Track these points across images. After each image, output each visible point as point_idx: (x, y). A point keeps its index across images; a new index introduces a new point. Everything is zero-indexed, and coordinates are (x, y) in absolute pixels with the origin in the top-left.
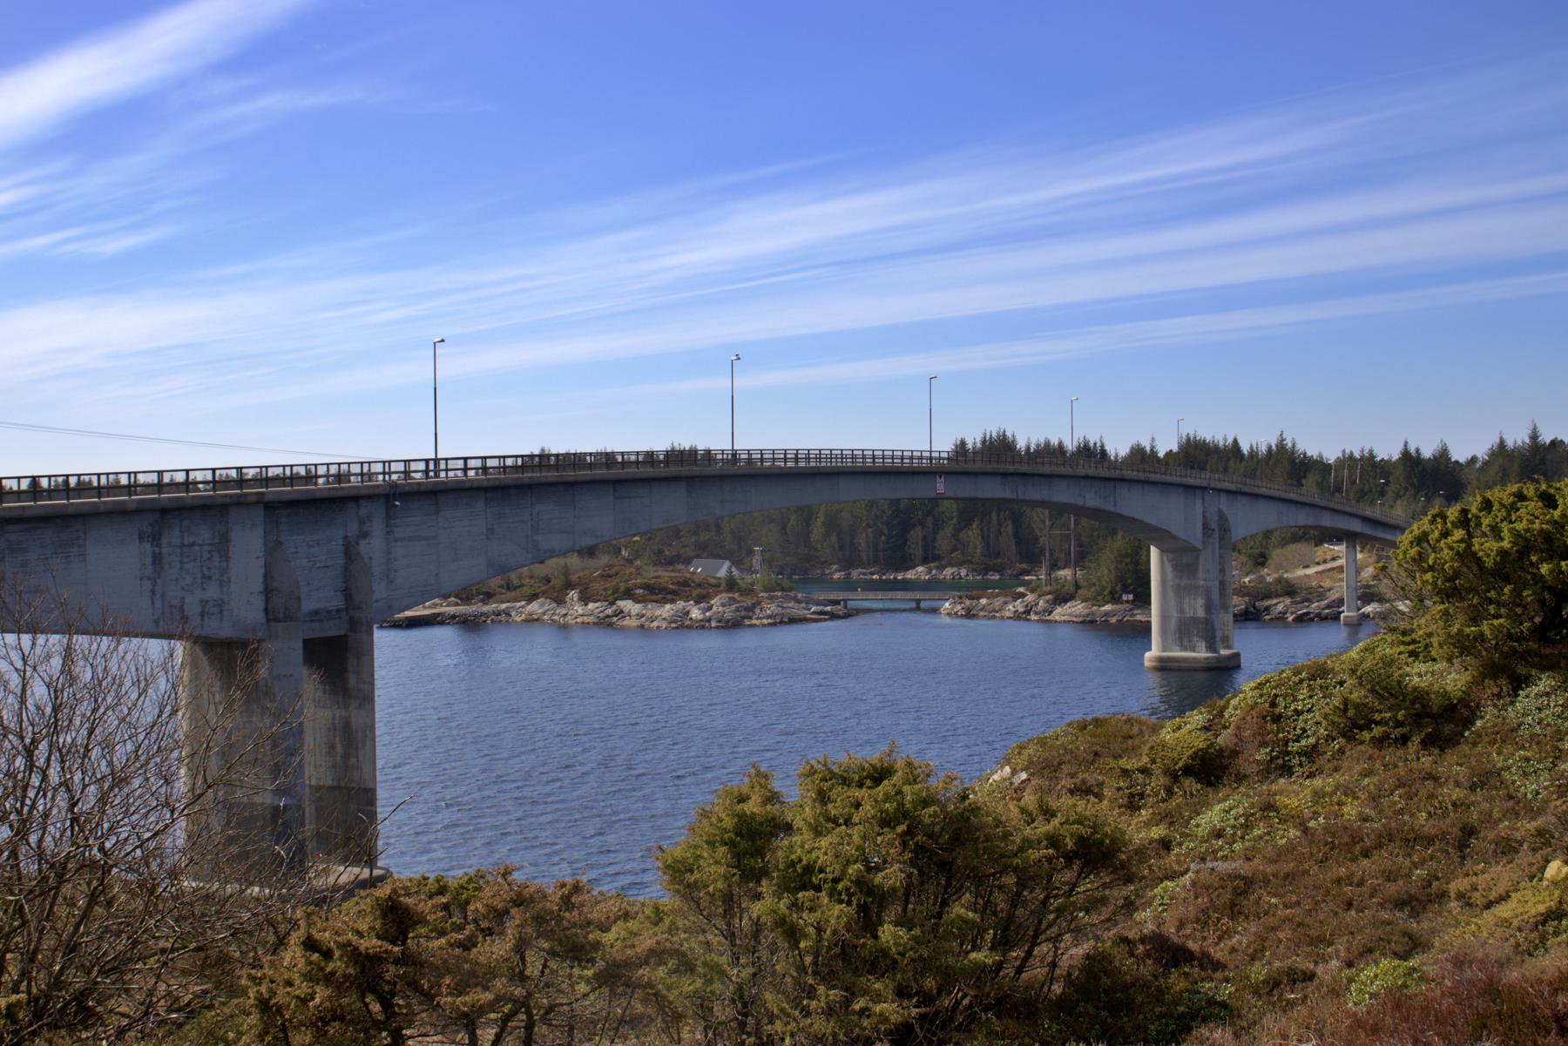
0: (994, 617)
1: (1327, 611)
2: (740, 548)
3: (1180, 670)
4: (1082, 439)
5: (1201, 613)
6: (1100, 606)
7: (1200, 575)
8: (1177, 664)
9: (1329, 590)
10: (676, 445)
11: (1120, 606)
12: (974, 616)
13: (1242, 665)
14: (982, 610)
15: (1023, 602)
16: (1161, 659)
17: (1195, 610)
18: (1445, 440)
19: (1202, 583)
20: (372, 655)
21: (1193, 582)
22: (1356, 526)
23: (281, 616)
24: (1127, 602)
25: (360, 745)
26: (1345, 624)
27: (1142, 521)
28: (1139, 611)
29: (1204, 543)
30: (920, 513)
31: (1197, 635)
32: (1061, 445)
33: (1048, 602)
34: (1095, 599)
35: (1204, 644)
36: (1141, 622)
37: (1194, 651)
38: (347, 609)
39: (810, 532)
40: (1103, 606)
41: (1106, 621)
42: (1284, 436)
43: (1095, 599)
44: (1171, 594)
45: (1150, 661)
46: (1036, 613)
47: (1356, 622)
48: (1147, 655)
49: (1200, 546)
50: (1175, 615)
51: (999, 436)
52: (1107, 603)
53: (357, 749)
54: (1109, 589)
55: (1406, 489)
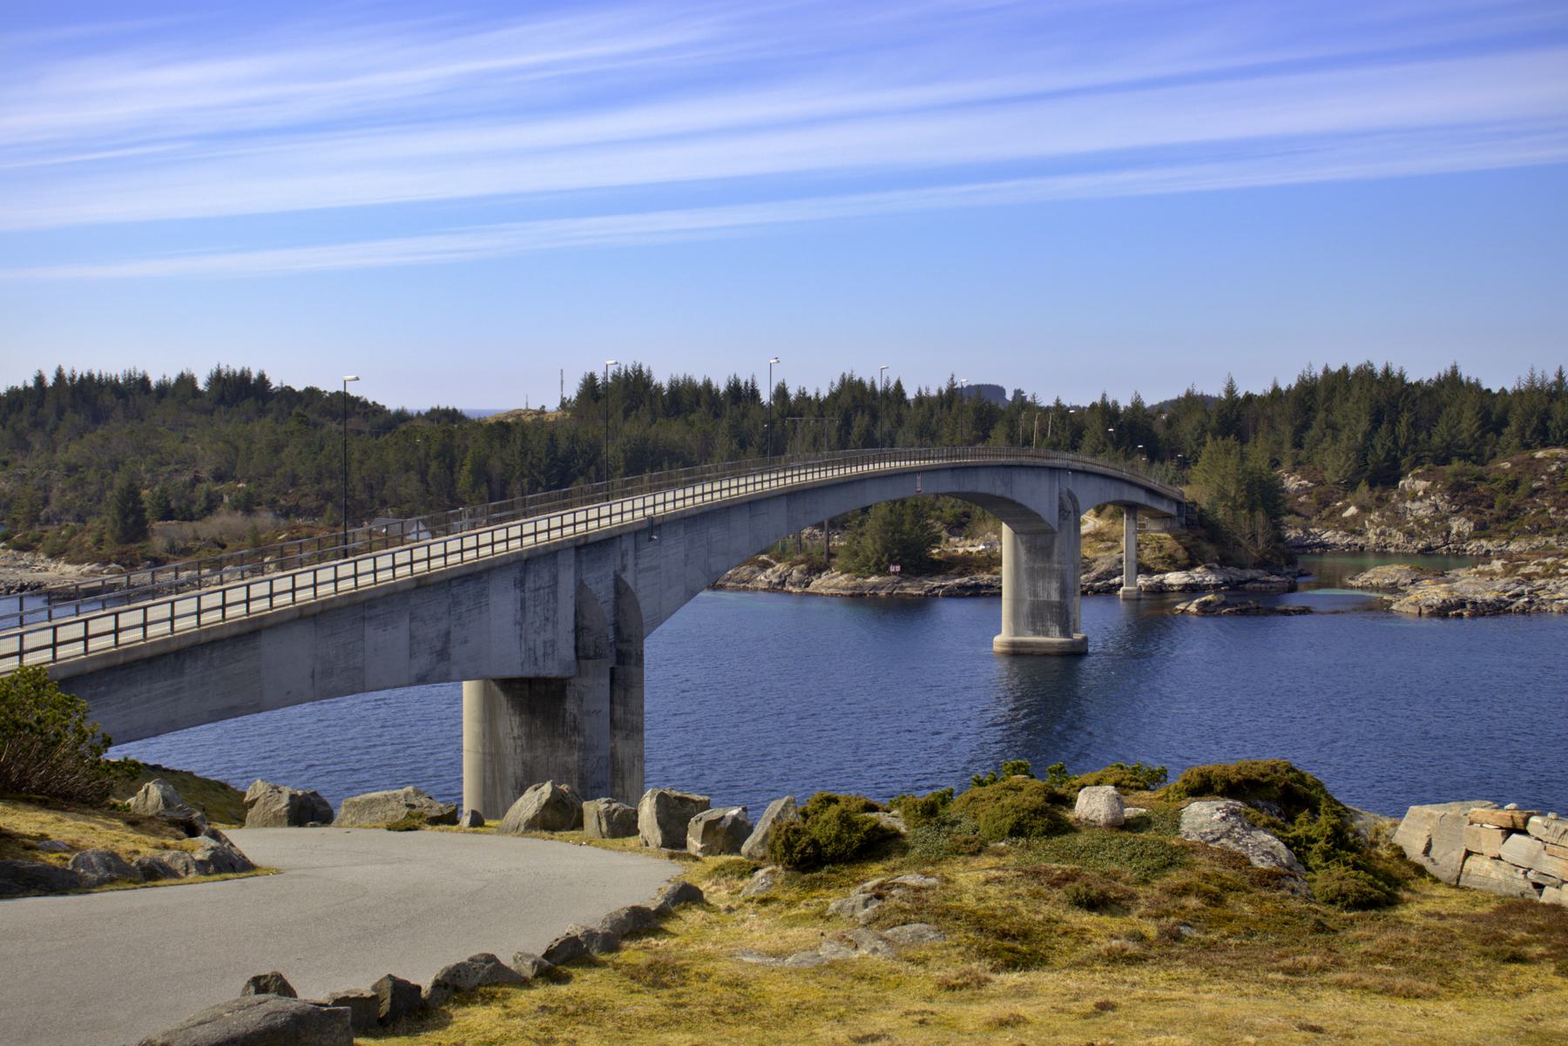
0: (745, 589)
2: (372, 497)
3: (1031, 655)
4: (732, 377)
5: (1055, 597)
6: (865, 578)
7: (1055, 558)
9: (1095, 561)
10: (223, 367)
12: (721, 587)
14: (729, 580)
15: (774, 572)
16: (1013, 644)
17: (1049, 594)
18: (1139, 392)
19: (1056, 566)
20: (642, 688)
22: (1140, 497)
23: (592, 653)
24: (895, 573)
25: (627, 775)
26: (1124, 599)
28: (908, 584)
29: (1059, 525)
30: (581, 461)
31: (1051, 620)
32: (708, 384)
33: (802, 572)
34: (858, 569)
35: (1058, 628)
37: (1047, 635)
39: (453, 483)
40: (868, 577)
41: (875, 594)
44: (1024, 577)
45: (1002, 646)
46: (793, 585)
48: (997, 639)
49: (1057, 529)
50: (1028, 598)
51: (634, 372)
53: (623, 778)
54: (875, 559)
55: (1105, 444)
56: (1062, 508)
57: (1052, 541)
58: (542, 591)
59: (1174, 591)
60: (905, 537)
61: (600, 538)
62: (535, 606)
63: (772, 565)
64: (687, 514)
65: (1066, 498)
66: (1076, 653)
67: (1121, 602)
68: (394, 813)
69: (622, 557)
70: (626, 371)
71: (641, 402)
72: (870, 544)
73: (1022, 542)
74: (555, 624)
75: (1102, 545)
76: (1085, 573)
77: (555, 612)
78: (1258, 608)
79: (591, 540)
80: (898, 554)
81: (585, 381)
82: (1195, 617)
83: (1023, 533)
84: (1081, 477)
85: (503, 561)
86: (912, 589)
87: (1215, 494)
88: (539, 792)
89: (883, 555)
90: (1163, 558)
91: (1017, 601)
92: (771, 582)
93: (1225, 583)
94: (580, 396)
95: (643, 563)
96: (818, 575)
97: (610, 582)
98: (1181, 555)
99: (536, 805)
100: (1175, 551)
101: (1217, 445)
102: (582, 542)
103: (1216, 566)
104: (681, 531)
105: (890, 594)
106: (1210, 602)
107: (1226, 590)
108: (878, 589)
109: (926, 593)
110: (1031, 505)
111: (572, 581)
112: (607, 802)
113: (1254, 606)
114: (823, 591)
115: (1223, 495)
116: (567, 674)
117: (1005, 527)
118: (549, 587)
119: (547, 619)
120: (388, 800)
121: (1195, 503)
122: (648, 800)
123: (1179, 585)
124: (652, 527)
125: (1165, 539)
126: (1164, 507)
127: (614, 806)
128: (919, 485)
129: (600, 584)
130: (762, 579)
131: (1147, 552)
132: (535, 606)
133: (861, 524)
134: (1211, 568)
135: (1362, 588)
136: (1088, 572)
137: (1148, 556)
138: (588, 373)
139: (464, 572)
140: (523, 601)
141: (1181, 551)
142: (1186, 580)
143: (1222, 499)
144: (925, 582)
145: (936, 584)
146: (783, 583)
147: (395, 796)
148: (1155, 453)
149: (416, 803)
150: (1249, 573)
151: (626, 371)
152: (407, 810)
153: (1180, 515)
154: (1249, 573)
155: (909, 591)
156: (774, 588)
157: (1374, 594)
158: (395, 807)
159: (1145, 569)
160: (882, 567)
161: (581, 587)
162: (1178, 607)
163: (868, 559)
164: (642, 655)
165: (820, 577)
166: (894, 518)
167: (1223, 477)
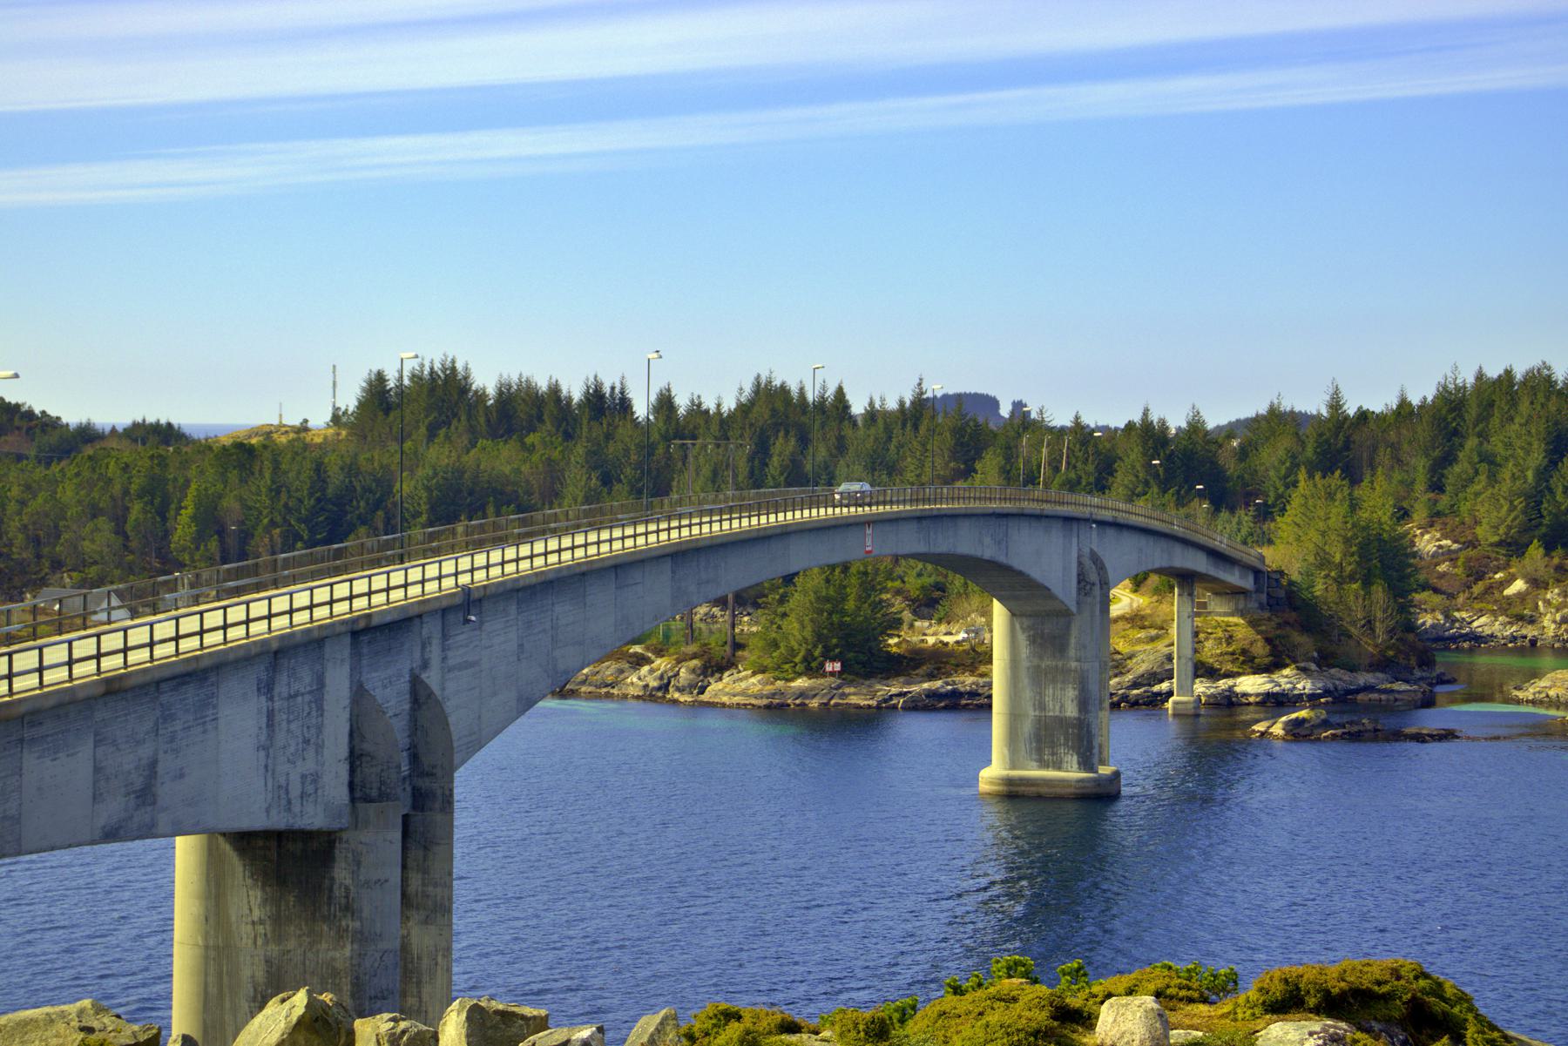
0: (608, 696)
1: (1135, 692)
2: (39, 556)
5: (1071, 711)
6: (788, 680)
7: (1072, 652)
8: (1033, 789)
9: (1130, 658)
11: (822, 681)
12: (573, 694)
13: (1125, 791)
14: (583, 682)
15: (652, 671)
16: (1009, 781)
18: (1199, 406)
19: (1073, 664)
21: (1060, 664)
22: (1199, 563)
23: (374, 793)
24: (832, 674)
25: (425, 978)
26: (1175, 715)
27: (1028, 576)
28: (852, 690)
29: (1078, 603)
30: (362, 504)
31: (1066, 744)
32: (555, 390)
33: (693, 671)
34: (778, 668)
35: (1075, 757)
36: (858, 707)
37: (1059, 768)
38: (410, 776)
39: (167, 534)
40: (792, 680)
41: (803, 704)
42: (924, 386)
43: (778, 668)
44: (1025, 681)
45: (991, 783)
47: (1192, 712)
49: (1074, 609)
50: (1032, 713)
51: (444, 369)
52: (800, 675)
53: (419, 983)
54: (802, 654)
56: (1082, 578)
57: (1068, 627)
58: (299, 699)
59: (1249, 704)
60: (848, 619)
61: (388, 619)
62: (289, 722)
63: (649, 661)
64: (522, 584)
65: (1087, 562)
66: (1103, 795)
67: (1170, 719)
68: (61, 1040)
69: (423, 647)
70: (432, 368)
71: (455, 415)
72: (796, 630)
73: (1021, 628)
74: (319, 748)
75: (1142, 634)
76: (1116, 676)
77: (320, 729)
78: (1376, 730)
79: (375, 621)
80: (836, 646)
81: (370, 383)
82: (1279, 744)
83: (1022, 615)
84: (1111, 532)
85: (241, 653)
86: (857, 697)
87: (1311, 559)
88: (287, 1004)
89: (815, 646)
90: (1233, 654)
91: (1014, 717)
92: (646, 686)
93: (1327, 692)
94: (362, 405)
95: (455, 657)
96: (717, 675)
97: (403, 685)
98: (1260, 649)
99: (282, 1025)
100: (1252, 644)
101: (1315, 486)
102: (362, 624)
103: (1313, 666)
104: (513, 609)
105: (826, 704)
106: (1304, 720)
107: (1327, 702)
108: (807, 697)
109: (879, 703)
110: (1036, 573)
111: (347, 683)
112: (392, 1020)
113: (1370, 727)
114: (725, 699)
115: (1323, 561)
116: (336, 825)
117: (997, 608)
118: (310, 692)
119: (306, 742)
120: (52, 1021)
121: (1281, 573)
122: (454, 1015)
123: (1257, 695)
124: (468, 604)
125: (1236, 625)
126: (1234, 578)
127: (403, 1025)
128: (869, 543)
129: (390, 693)
130: (636, 680)
131: (1209, 644)
132: (289, 722)
133: (783, 600)
134: (1304, 670)
135: (1533, 702)
136: (1121, 674)
137: (1211, 651)
138: (375, 370)
139: (179, 670)
140: (270, 715)
141: (1260, 644)
142: (1268, 687)
143: (1321, 566)
144: (878, 687)
145: (894, 690)
146: (665, 687)
147: (63, 1015)
148: (1221, 498)
149: (96, 1024)
150: (1363, 678)
151: (432, 368)
152: (82, 1035)
153: (1258, 591)
154: (1363, 678)
155: (854, 700)
156: (651, 695)
157: (1553, 712)
158: (62, 1031)
159: (1204, 670)
160: (814, 665)
161: (359, 694)
162: (1256, 728)
163: (792, 652)
164: (451, 795)
165: (721, 679)
166: (832, 592)
167: (1323, 534)
